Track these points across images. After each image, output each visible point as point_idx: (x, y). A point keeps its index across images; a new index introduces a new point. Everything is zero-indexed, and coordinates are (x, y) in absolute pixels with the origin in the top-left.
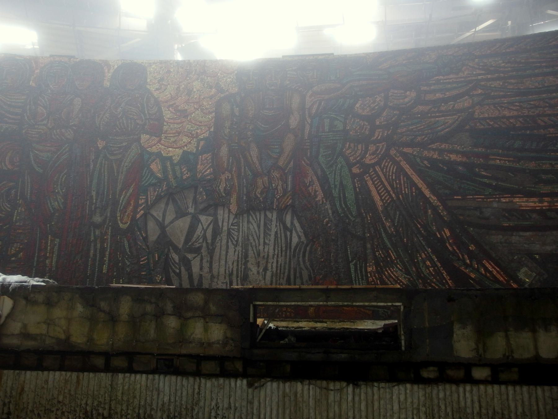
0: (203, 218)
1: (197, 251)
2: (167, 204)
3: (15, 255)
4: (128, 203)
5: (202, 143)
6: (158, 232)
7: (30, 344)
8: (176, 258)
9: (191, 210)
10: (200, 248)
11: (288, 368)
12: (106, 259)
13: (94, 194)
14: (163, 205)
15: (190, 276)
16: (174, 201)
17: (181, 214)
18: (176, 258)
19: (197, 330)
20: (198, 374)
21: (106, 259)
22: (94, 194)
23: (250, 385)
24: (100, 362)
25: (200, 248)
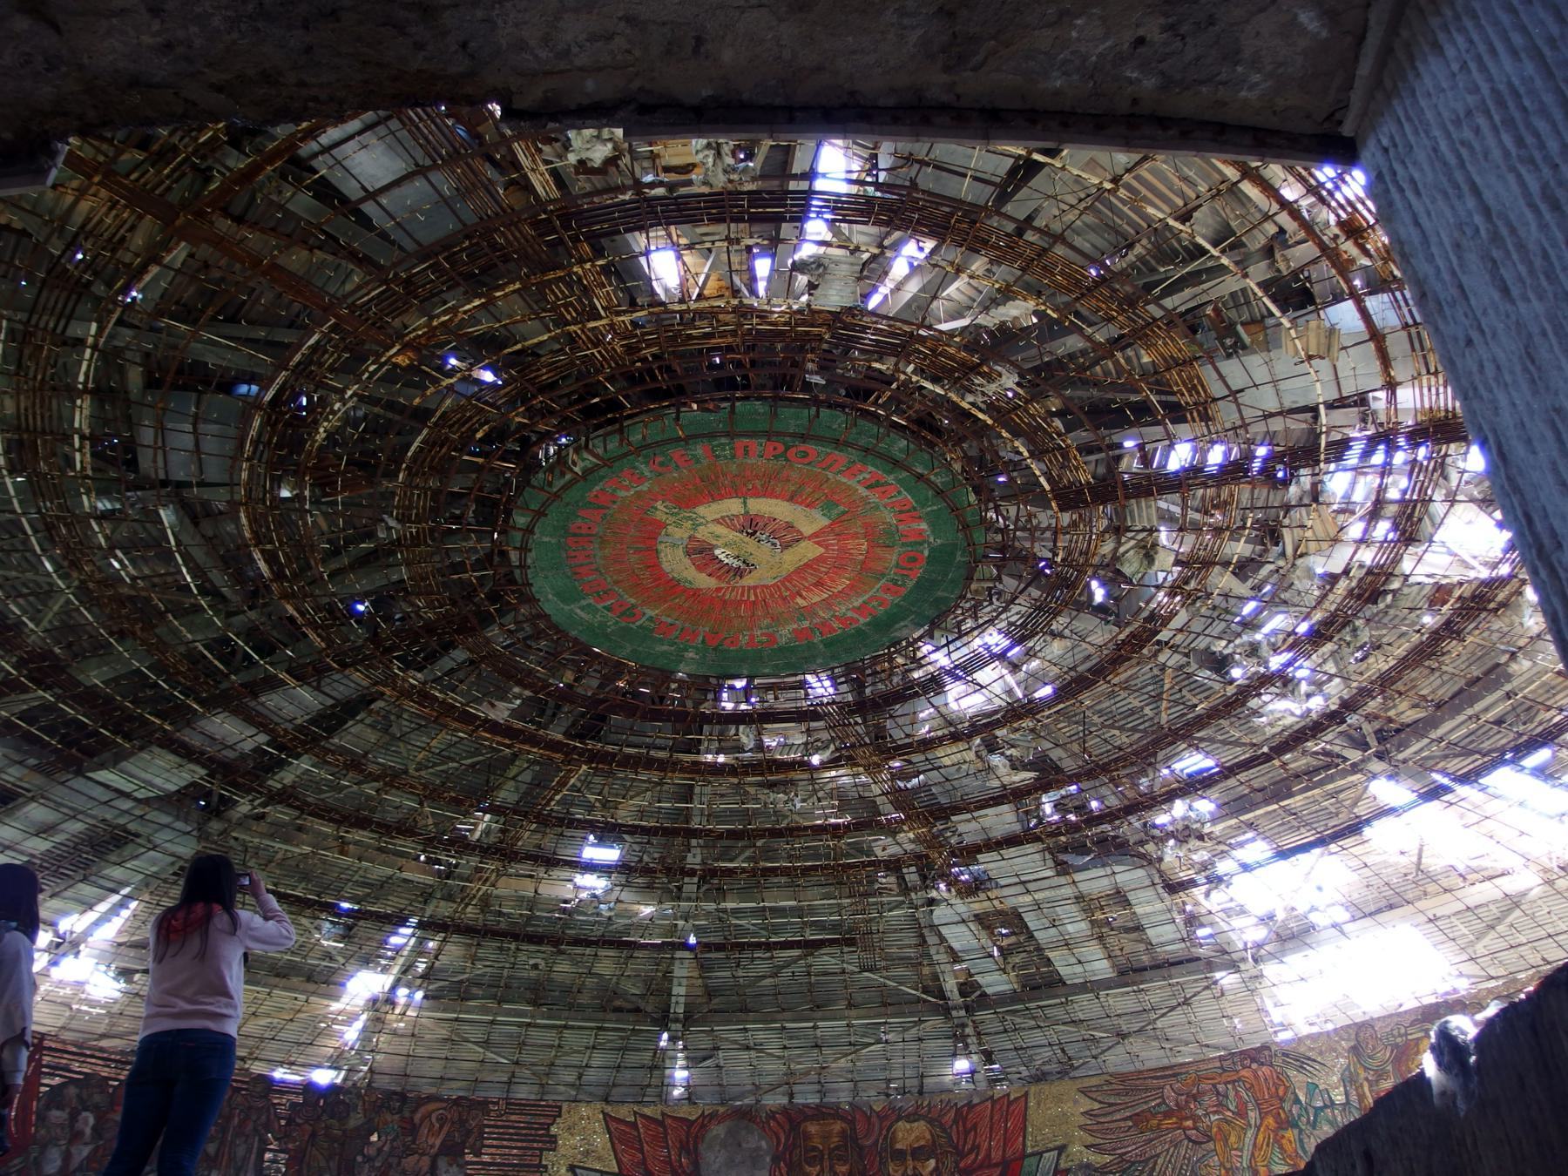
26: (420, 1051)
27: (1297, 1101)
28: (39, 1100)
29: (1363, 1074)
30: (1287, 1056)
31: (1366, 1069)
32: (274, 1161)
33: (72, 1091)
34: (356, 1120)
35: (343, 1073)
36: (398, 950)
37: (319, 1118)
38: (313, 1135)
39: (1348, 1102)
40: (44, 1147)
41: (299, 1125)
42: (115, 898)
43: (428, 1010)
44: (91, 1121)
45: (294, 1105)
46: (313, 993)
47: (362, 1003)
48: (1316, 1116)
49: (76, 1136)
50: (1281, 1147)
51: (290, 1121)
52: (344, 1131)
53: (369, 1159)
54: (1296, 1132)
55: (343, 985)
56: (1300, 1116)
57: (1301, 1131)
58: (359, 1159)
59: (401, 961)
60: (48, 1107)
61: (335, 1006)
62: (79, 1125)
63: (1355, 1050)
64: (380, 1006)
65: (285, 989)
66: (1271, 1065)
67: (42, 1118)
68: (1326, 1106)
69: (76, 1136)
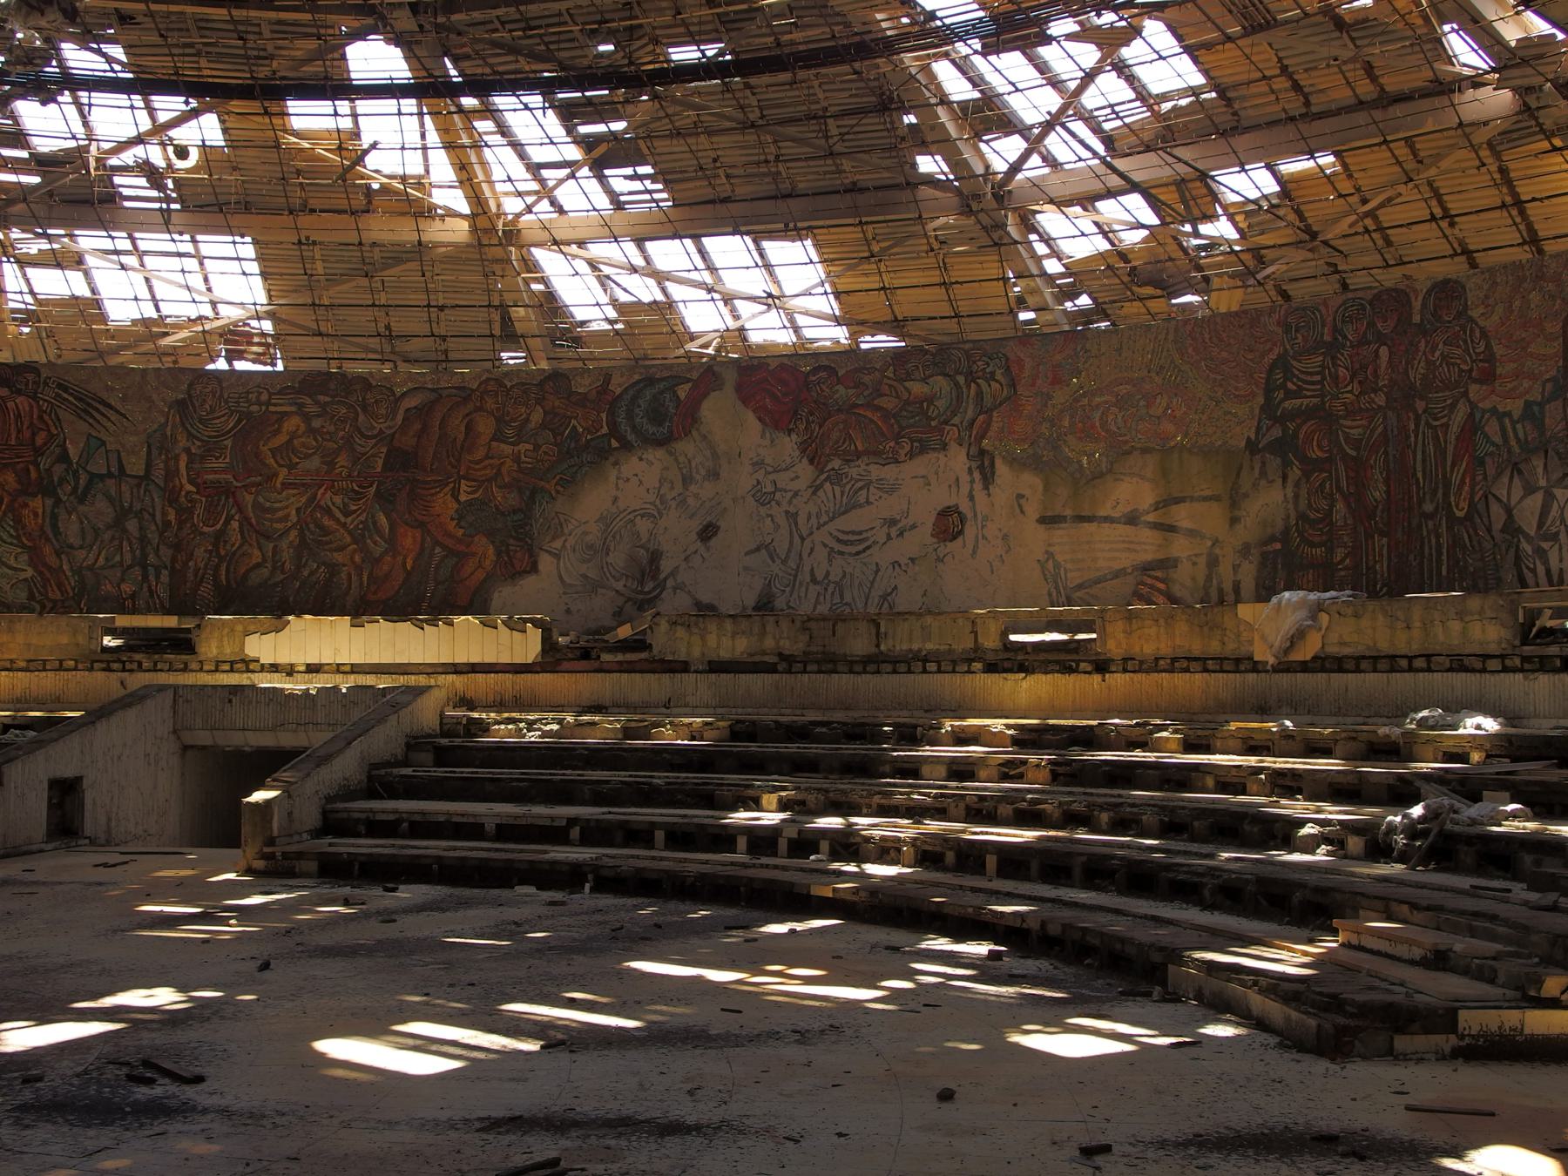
0: (1558, 492)
1: (1554, 537)
2: (1512, 477)
3: (1342, 561)
4: (1463, 482)
5: (1549, 386)
6: (1504, 517)
7: (1347, 651)
8: (1529, 549)
9: (1543, 483)
10: (1557, 534)
11: (1558, 663)
12: (1444, 558)
13: (1420, 475)
14: (1506, 480)
15: (1548, 572)
16: (1520, 472)
17: (1530, 490)
18: (1529, 549)
19: (1476, 631)
20: (1484, 671)
21: (1444, 558)
22: (1420, 475)
23: (1526, 678)
24: (1404, 663)
25: (1557, 534)
27: (64, 457)
29: (183, 442)
30: (66, 390)
31: (190, 436)
39: (147, 475)
48: (88, 488)
50: (18, 521)
54: (49, 502)
56: (62, 480)
57: (58, 502)
63: (182, 406)
66: (35, 398)
68: (110, 475)
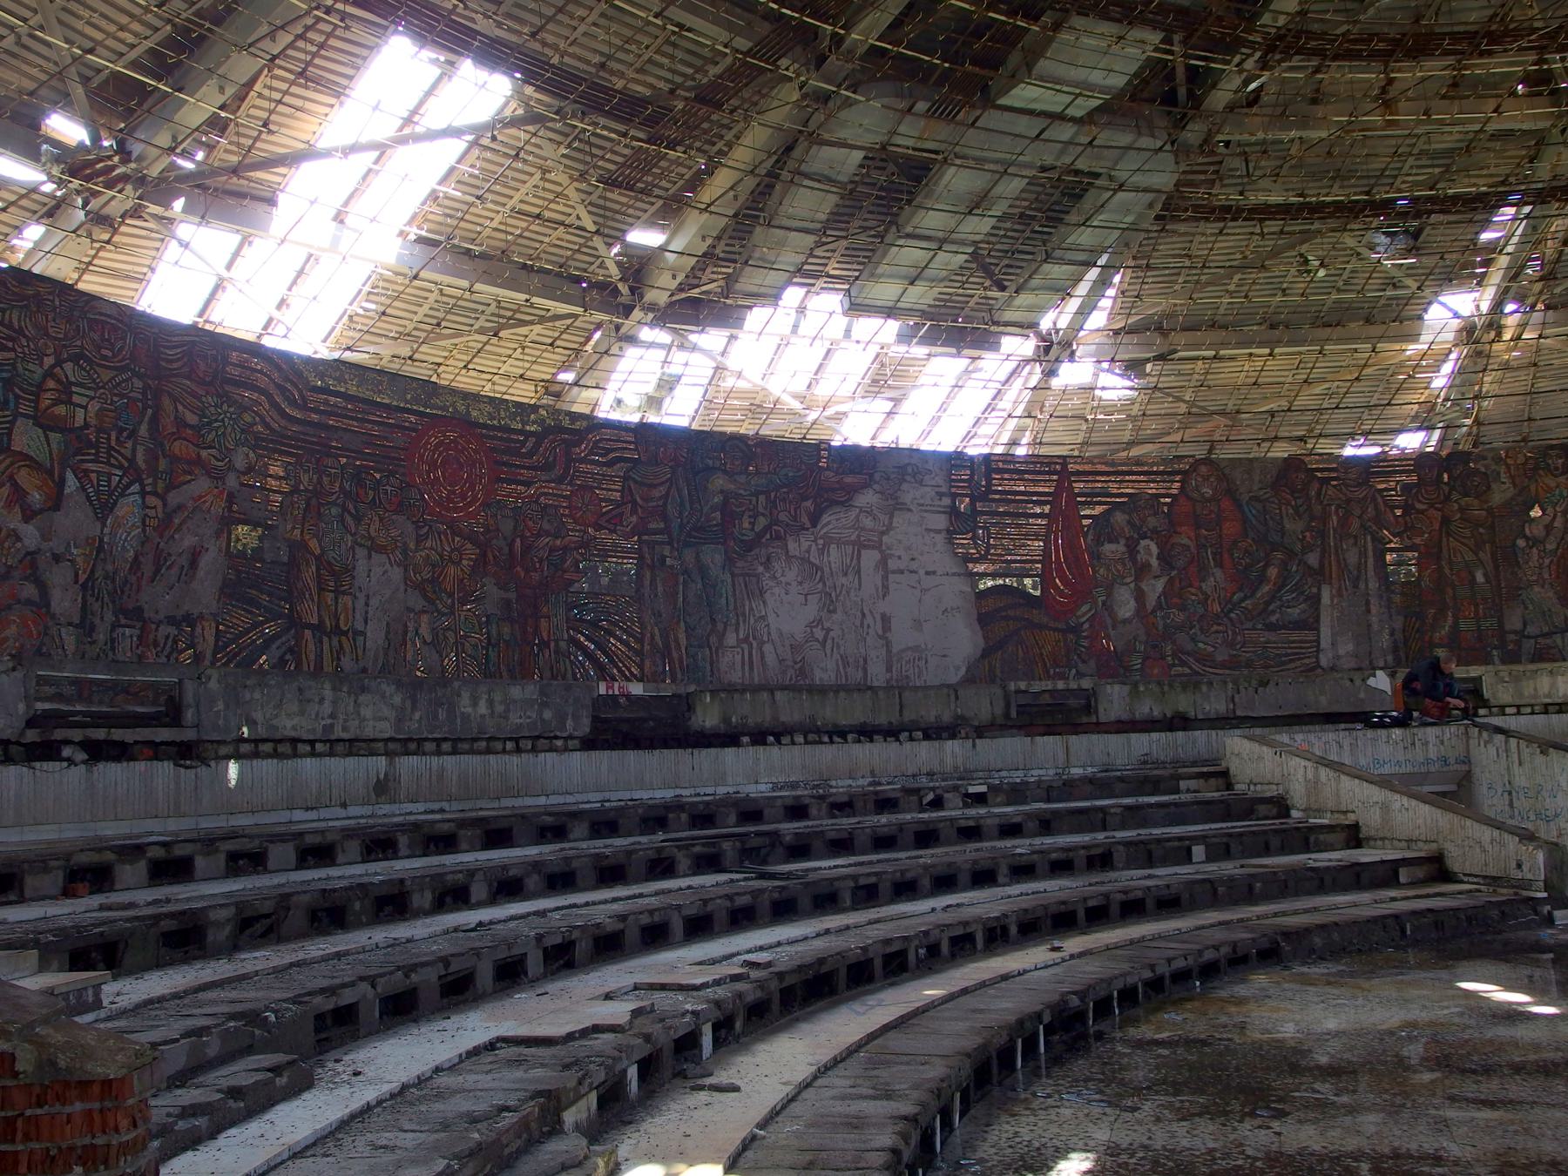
26: (1543, 385)
28: (1085, 535)
32: (1398, 563)
33: (1120, 518)
34: (1500, 494)
35: (1437, 434)
36: (1494, 248)
37: (1448, 498)
38: (1446, 521)
40: (1109, 589)
41: (1422, 512)
42: (1093, 273)
43: (1556, 324)
44: (1154, 549)
45: (1407, 488)
46: (1381, 338)
47: (1450, 336)
49: (1142, 570)
51: (1407, 509)
52: (1490, 511)
53: (1534, 542)
55: (1420, 318)
58: (1521, 543)
59: (1503, 261)
60: (1098, 541)
61: (1412, 349)
62: (1141, 557)
64: (1475, 335)
65: (1340, 341)
67: (1096, 556)
69: (1142, 570)
